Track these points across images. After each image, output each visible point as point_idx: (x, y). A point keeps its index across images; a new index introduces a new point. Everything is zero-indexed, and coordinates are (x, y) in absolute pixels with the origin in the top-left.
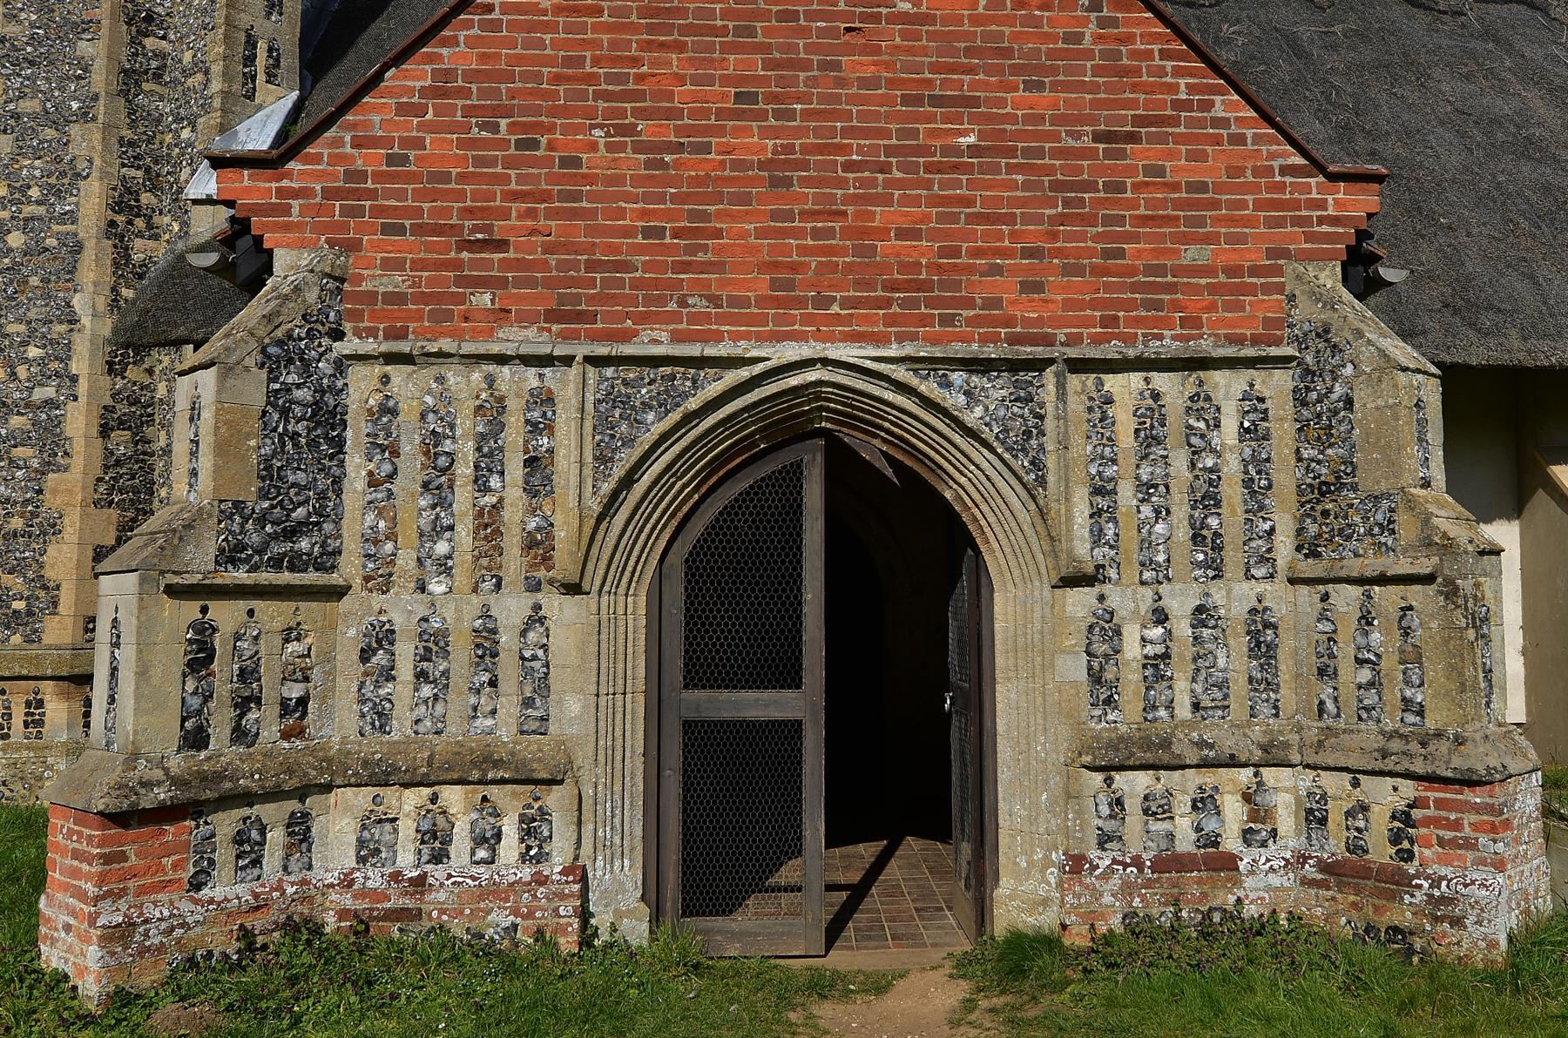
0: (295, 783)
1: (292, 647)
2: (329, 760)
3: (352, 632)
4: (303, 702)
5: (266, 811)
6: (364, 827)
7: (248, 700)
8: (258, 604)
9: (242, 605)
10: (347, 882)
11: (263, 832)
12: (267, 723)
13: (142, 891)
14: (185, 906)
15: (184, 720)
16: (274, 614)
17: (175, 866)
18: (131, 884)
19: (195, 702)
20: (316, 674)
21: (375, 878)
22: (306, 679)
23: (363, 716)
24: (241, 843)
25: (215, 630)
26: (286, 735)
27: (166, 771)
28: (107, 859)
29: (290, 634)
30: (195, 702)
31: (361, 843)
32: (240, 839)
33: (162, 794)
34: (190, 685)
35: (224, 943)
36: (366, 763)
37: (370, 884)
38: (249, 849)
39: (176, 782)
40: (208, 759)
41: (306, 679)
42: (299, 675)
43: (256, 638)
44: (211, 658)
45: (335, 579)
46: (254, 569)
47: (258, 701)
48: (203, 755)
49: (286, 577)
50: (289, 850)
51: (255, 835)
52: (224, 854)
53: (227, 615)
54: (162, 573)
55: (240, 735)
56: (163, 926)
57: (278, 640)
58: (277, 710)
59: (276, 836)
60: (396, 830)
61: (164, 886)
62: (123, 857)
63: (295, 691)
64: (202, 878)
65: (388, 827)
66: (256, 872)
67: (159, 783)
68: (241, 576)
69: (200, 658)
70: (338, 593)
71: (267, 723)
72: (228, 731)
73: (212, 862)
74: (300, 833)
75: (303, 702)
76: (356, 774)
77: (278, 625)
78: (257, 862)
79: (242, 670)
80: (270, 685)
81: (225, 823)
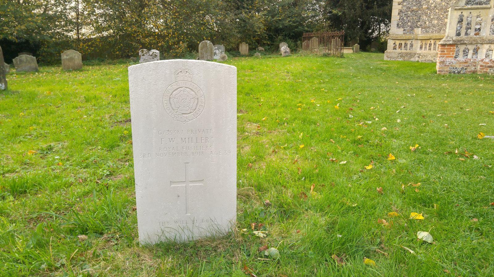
0: (475, 43)
1: (479, 19)
2: (483, 39)
3: (491, 16)
4: (479, 29)
5: (469, 47)
6: (487, 51)
7: (468, 28)
8: (471, 11)
9: (469, 11)
10: (482, 60)
11: (468, 50)
12: (472, 33)
13: (447, 57)
14: (453, 60)
15: (457, 31)
16: (475, 13)
17: (452, 54)
18: (445, 56)
19: (459, 28)
20: (483, 24)
21: (487, 60)
22: (481, 25)
23: (490, 31)
24: (464, 52)
25: (463, 16)
26: (476, 35)
27: (452, 39)
28: (442, 51)
29: (478, 17)
30: (459, 28)
31: (486, 54)
32: (464, 51)
33: (451, 42)
34: (458, 25)
35: (459, 67)
36: (489, 40)
37: (486, 61)
38: (465, 53)
39: (453, 41)
40: (460, 38)
41: (481, 25)
42: (479, 24)
43: (471, 17)
44: (462, 21)
45: (489, 6)
46: (472, 5)
47: (470, 28)
48: (459, 37)
49: (479, 6)
50: (473, 54)
51: (467, 51)
52: (461, 53)
53: (466, 13)
54: (455, 7)
55: (466, 34)
56: (449, 62)
57: (476, 18)
58: (474, 30)
59: (471, 52)
60: (492, 52)
61: (451, 57)
62: (444, 51)
63: (478, 27)
64: (457, 56)
65: (491, 51)
66: (467, 57)
67: (451, 41)
68: (469, 6)
69: (461, 21)
70: (490, 8)
71: (472, 33)
72: (464, 33)
73: (459, 54)
74: (476, 51)
75: (479, 29)
76: (487, 42)
77: (476, 15)
78: (467, 55)
79: (468, 23)
80: (474, 26)
81: (462, 48)
